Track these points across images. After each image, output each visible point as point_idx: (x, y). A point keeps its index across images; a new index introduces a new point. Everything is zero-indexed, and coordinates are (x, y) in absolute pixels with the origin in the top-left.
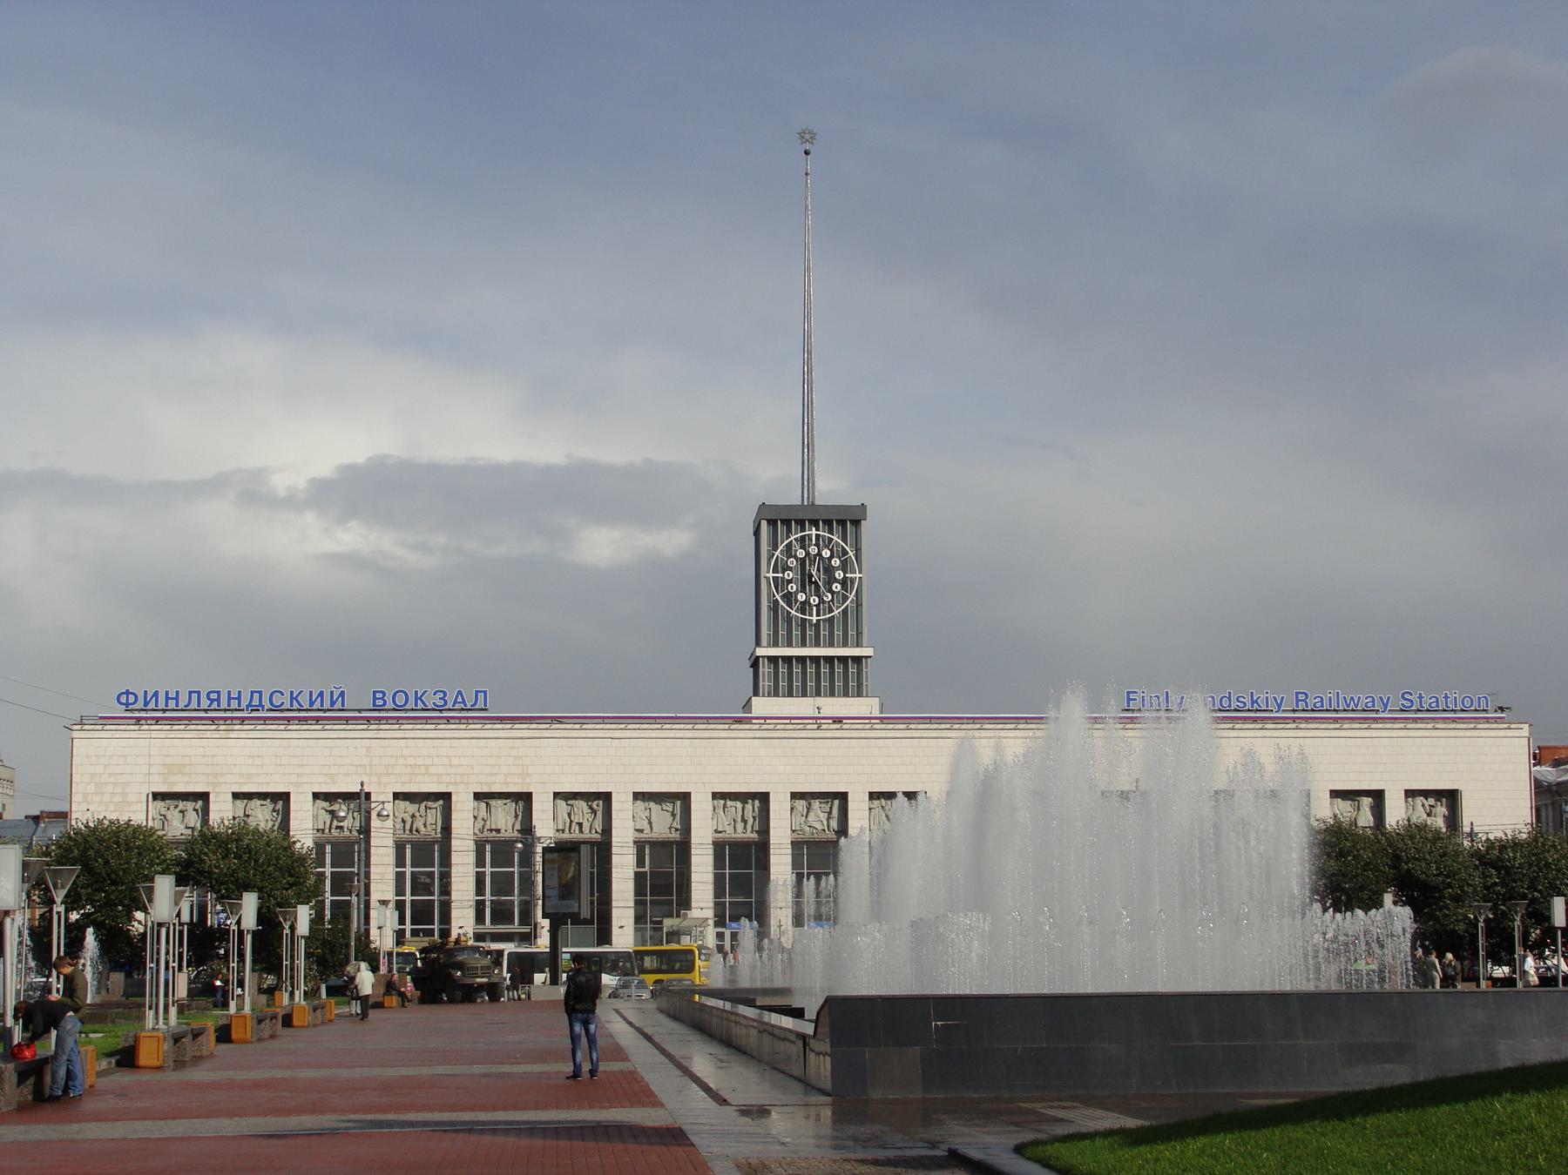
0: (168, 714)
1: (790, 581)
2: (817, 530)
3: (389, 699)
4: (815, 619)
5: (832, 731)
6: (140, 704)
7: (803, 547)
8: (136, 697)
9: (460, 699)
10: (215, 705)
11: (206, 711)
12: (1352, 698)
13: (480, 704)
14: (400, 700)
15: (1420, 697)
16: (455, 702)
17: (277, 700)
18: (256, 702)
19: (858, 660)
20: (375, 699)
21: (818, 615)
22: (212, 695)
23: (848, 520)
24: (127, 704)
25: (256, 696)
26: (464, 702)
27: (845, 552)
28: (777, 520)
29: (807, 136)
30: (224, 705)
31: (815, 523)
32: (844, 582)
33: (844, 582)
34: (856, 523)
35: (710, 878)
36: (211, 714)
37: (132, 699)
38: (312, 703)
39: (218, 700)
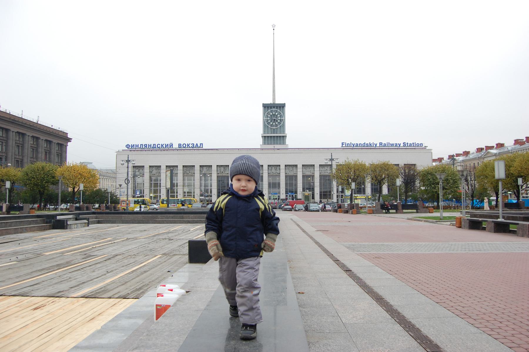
0: (136, 149)
1: (269, 120)
2: (275, 109)
3: (182, 145)
4: (274, 128)
6: (130, 147)
7: (272, 112)
9: (197, 145)
10: (146, 147)
11: (144, 148)
12: (392, 144)
13: (201, 147)
14: (184, 146)
15: (407, 144)
16: (196, 146)
17: (159, 146)
18: (154, 146)
20: (179, 146)
21: (275, 127)
22: (146, 145)
23: (282, 106)
24: (128, 147)
25: (154, 145)
26: (198, 146)
27: (281, 114)
28: (266, 107)
30: (148, 147)
31: (274, 107)
32: (280, 120)
33: (280, 120)
34: (284, 107)
35: (284, 183)
36: (145, 149)
38: (166, 147)
39: (147, 146)
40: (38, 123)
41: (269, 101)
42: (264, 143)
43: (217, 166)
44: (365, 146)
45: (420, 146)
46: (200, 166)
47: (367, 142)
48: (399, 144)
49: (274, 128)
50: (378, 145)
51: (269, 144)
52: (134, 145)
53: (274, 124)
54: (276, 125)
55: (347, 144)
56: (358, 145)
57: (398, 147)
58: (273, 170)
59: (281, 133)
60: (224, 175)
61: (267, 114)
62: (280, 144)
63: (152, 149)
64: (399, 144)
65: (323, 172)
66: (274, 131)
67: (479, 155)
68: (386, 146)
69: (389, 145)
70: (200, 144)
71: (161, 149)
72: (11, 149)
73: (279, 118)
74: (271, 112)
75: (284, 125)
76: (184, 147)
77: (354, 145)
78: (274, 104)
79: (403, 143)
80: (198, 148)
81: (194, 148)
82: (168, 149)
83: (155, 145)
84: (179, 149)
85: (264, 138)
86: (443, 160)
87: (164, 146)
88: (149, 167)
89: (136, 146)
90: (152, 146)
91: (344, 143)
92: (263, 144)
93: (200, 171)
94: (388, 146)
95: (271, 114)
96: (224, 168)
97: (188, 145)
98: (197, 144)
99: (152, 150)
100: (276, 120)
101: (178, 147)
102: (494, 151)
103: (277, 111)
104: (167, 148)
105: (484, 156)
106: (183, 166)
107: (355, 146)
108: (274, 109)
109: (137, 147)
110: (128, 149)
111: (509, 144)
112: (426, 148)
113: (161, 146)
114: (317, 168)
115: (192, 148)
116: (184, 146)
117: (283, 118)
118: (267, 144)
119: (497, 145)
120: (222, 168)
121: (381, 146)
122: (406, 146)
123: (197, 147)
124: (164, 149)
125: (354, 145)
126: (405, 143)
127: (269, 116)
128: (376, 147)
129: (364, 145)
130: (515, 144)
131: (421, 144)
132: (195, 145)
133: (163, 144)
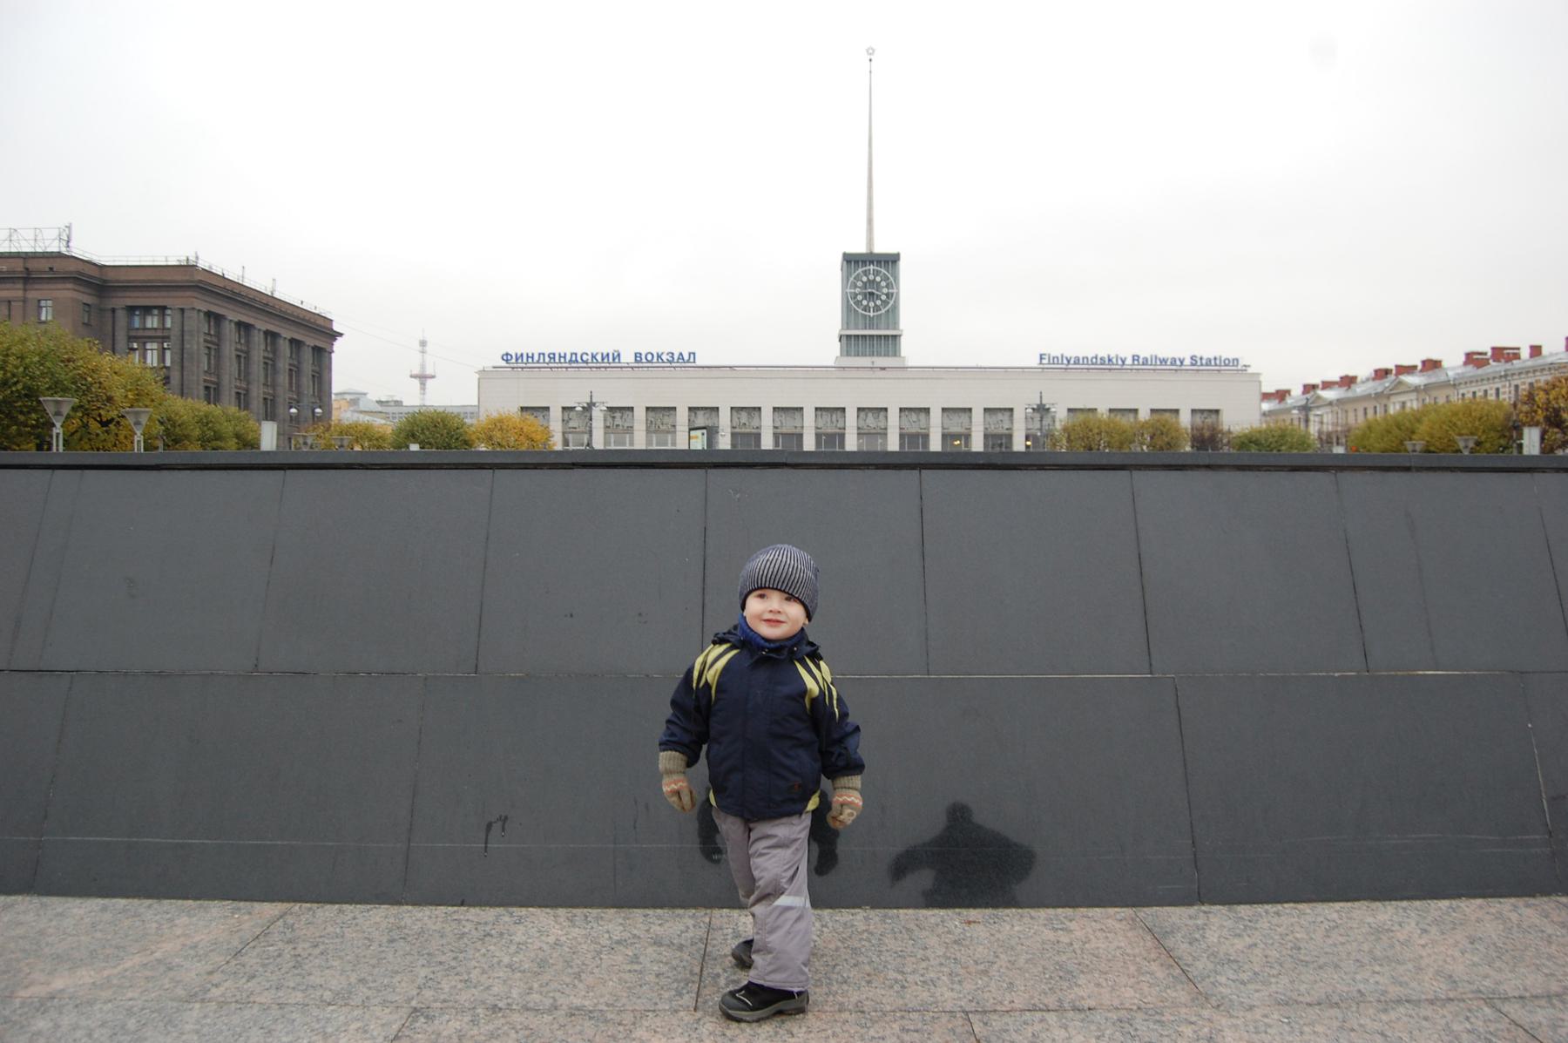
3: (643, 357)
6: (514, 361)
7: (866, 275)
8: (511, 356)
10: (552, 361)
13: (692, 360)
14: (649, 357)
16: (679, 358)
17: (585, 357)
18: (574, 358)
19: (895, 337)
20: (636, 357)
22: (552, 356)
23: (891, 261)
24: (507, 360)
25: (574, 356)
26: (683, 359)
27: (888, 278)
28: (851, 261)
29: (871, 51)
30: (557, 360)
31: (871, 262)
32: (887, 295)
33: (887, 295)
36: (551, 365)
38: (603, 359)
39: (554, 358)
40: (275, 296)
41: (860, 248)
42: (846, 352)
43: (732, 408)
44: (1096, 364)
45: (1231, 364)
46: (690, 409)
47: (1103, 353)
48: (1180, 360)
50: (1129, 361)
51: (858, 355)
52: (522, 355)
53: (872, 304)
54: (877, 308)
55: (1054, 358)
56: (1079, 360)
57: (1178, 368)
58: (871, 420)
59: (888, 329)
60: (748, 430)
61: (855, 278)
62: (885, 355)
63: (567, 365)
64: (1180, 360)
65: (993, 427)
66: (870, 323)
67: (1379, 386)
68: (1149, 363)
69: (1156, 362)
70: (690, 354)
71: (590, 365)
72: (228, 364)
73: (885, 290)
74: (866, 273)
75: (895, 308)
76: (651, 362)
77: (1069, 361)
78: (871, 254)
79: (1192, 358)
80: (683, 365)
81: (673, 365)
82: (608, 365)
83: (576, 354)
84: (636, 365)
85: (847, 340)
86: (1290, 394)
87: (599, 358)
88: (561, 409)
89: (528, 357)
90: (568, 358)
91: (1045, 355)
92: (841, 355)
93: (689, 420)
94: (1154, 363)
95: (865, 279)
96: (749, 414)
97: (659, 356)
98: (681, 354)
100: (877, 295)
101: (633, 361)
102: (1412, 380)
103: (877, 273)
104: (607, 362)
105: (1391, 390)
106: (647, 408)
107: (1072, 362)
109: (530, 360)
110: (507, 365)
111: (1453, 362)
112: (1245, 370)
113: (590, 357)
114: (936, 418)
115: (669, 365)
116: (649, 357)
118: (855, 356)
119: (1424, 362)
120: (744, 415)
121: (1136, 362)
122: (1199, 363)
123: (681, 361)
124: (598, 365)
125: (1069, 361)
126: (1195, 356)
127: (860, 284)
128: (1125, 367)
129: (1094, 360)
130: (1466, 363)
131: (1233, 360)
132: (676, 357)
133: (597, 354)
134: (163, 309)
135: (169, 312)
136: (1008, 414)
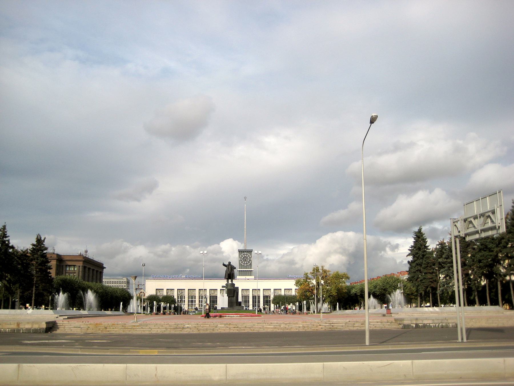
4: (245, 265)
5: (248, 281)
31: (245, 252)
33: (249, 260)
37: (153, 276)
49: (245, 265)
53: (245, 263)
54: (247, 263)
73: (249, 259)
99: (168, 279)
108: (245, 253)
117: (251, 259)
134: (74, 266)
135: (75, 266)
136: (280, 290)
